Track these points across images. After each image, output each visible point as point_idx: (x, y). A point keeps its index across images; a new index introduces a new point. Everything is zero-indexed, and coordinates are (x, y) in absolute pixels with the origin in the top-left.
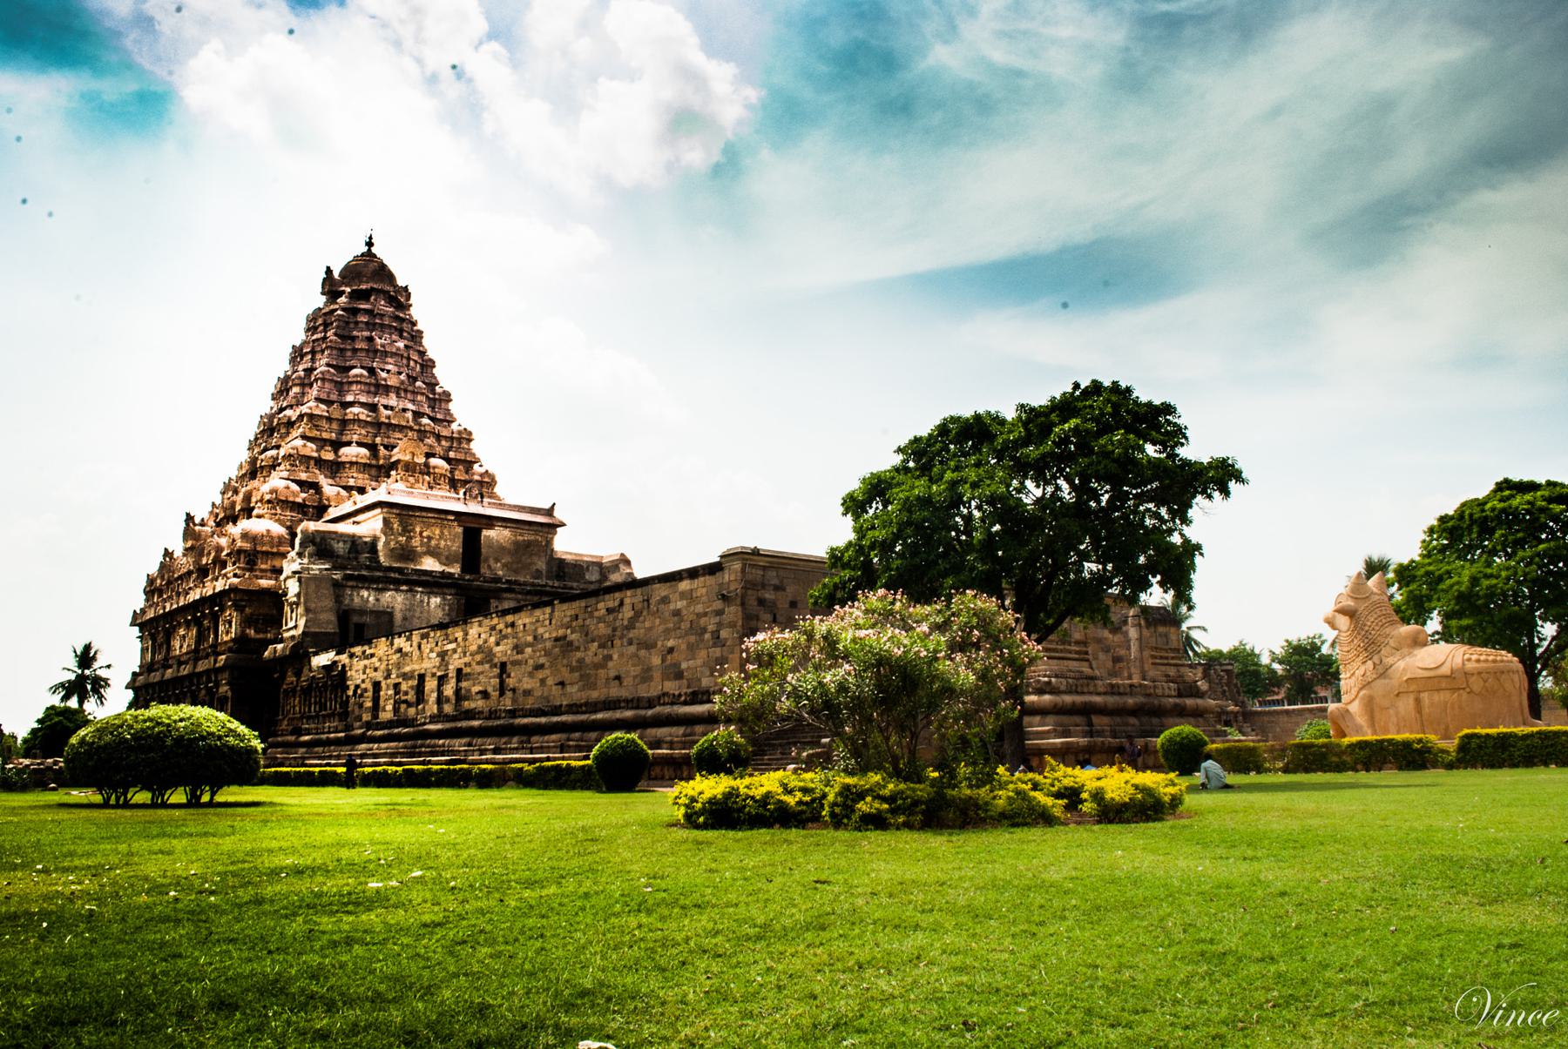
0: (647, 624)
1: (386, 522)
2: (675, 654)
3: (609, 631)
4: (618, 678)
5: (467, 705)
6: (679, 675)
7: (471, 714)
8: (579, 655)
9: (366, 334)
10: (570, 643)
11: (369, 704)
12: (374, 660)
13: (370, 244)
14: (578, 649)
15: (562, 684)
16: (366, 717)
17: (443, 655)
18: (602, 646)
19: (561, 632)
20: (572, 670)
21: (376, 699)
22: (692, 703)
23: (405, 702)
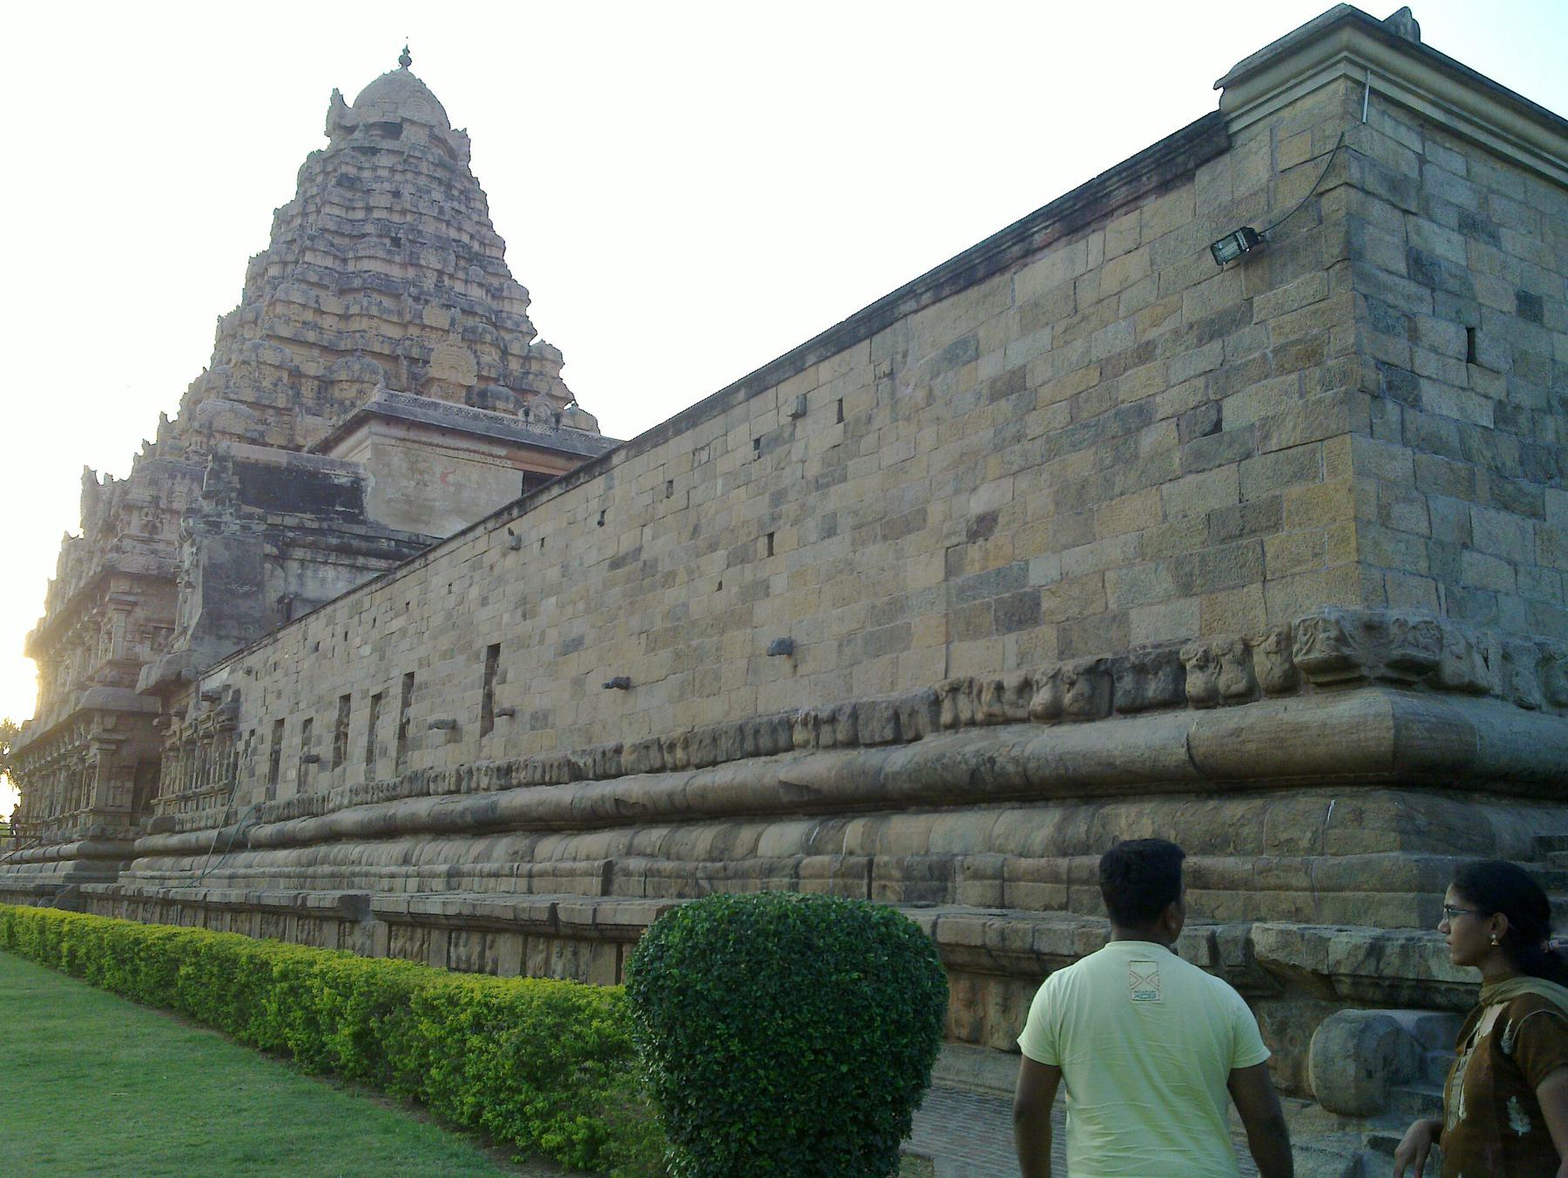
0: (889, 456)
1: (378, 452)
2: (1000, 536)
3: (763, 506)
4: (786, 648)
5: (420, 760)
6: (1021, 612)
7: (419, 786)
8: (672, 596)
9: (387, 186)
10: (649, 568)
11: (264, 768)
13: (405, 60)
14: (669, 578)
15: (624, 685)
16: (258, 796)
17: (381, 651)
19: (626, 544)
20: (654, 643)
22: (1087, 714)
23: (315, 759)
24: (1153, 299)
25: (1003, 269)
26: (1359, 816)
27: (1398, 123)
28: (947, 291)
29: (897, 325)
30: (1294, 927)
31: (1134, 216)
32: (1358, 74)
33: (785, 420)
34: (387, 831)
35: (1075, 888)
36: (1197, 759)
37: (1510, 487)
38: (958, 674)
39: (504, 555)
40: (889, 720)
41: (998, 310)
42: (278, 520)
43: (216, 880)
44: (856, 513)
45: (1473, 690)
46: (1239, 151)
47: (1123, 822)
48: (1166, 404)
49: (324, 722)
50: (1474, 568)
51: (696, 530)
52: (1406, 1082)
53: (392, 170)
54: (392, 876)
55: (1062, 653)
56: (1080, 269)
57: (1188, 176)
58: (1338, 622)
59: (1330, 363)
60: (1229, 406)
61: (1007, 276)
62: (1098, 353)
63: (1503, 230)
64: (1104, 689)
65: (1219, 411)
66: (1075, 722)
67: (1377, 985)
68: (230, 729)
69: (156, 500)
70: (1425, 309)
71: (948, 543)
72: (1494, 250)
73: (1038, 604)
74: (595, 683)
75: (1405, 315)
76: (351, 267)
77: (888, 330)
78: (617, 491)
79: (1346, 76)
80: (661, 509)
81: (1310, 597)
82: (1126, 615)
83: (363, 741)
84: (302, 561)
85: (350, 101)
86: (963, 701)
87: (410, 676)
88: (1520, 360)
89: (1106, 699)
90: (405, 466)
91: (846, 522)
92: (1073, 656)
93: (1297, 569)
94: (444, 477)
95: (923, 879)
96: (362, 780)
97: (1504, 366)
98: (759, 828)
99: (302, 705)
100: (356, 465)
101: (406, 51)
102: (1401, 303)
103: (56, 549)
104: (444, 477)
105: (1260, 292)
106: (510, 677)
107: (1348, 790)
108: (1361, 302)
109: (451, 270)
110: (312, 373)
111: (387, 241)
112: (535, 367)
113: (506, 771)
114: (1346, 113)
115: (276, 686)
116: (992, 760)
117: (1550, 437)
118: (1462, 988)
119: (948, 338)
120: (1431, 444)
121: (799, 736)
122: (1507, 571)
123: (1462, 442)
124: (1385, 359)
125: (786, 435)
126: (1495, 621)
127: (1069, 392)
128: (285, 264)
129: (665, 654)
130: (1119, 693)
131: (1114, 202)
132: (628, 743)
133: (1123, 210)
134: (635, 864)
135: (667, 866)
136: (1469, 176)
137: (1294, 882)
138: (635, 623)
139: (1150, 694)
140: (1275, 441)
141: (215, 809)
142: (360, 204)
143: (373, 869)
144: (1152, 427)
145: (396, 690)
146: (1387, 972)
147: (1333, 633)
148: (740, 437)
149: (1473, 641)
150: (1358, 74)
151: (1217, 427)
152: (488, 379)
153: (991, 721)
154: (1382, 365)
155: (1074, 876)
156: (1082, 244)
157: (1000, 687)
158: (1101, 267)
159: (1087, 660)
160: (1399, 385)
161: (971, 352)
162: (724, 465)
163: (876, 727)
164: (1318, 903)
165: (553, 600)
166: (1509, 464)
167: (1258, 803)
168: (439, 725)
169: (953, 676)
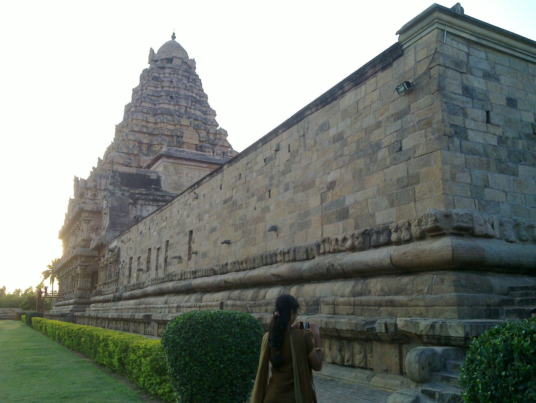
1: (165, 167)
2: (337, 189)
3: (267, 181)
4: (274, 229)
6: (343, 215)
7: (170, 278)
8: (241, 212)
9: (168, 79)
10: (235, 203)
11: (127, 273)
12: (131, 242)
13: (174, 37)
15: (228, 242)
16: (126, 283)
17: (159, 233)
18: (261, 199)
19: (228, 196)
21: (130, 271)
22: (363, 248)
24: (380, 107)
25: (336, 99)
26: (442, 281)
27: (458, 42)
28: (319, 107)
29: (305, 119)
30: (409, 319)
31: (374, 79)
32: (442, 27)
33: (273, 152)
34: (161, 293)
35: (356, 307)
36: (394, 263)
37: (504, 166)
38: (325, 236)
39: (193, 200)
40: (305, 252)
41: (334, 112)
42: (133, 191)
43: (112, 311)
44: (294, 182)
45: (487, 236)
46: (406, 55)
47: (372, 285)
48: (386, 141)
49: (144, 256)
50: (489, 194)
51: (248, 191)
52: (439, 371)
53: (170, 74)
54: (161, 308)
55: (356, 228)
56: (359, 98)
57: (390, 64)
58: (435, 215)
59: (434, 126)
60: (404, 141)
61: (337, 101)
62: (365, 126)
63: (501, 77)
64: (367, 240)
65: (401, 143)
66: (359, 251)
67: (434, 338)
68: (117, 261)
69: (95, 186)
70: (469, 105)
71: (321, 192)
72: (497, 84)
73: (348, 211)
74: (219, 243)
75: (461, 108)
76: (157, 107)
77: (303, 121)
78: (225, 178)
79: (438, 28)
80: (238, 183)
81: (428, 205)
82: (374, 214)
83: (155, 263)
84: (141, 205)
85: (156, 52)
86: (326, 245)
87: (168, 241)
88: (508, 122)
89: (368, 243)
90: (174, 172)
91: (291, 186)
92: (359, 229)
93: (425, 197)
94: (187, 175)
95: (312, 306)
96: (155, 276)
97: (501, 123)
98: (267, 289)
99: (137, 252)
100: (158, 172)
101: (174, 34)
102: (460, 104)
103: (67, 203)
104: (187, 175)
105: (413, 103)
106: (196, 240)
107: (442, 272)
108: (444, 105)
109: (190, 106)
110: (145, 142)
111: (169, 98)
112: (218, 136)
113: (195, 272)
114: (438, 40)
115: (130, 246)
116: (333, 265)
117: (520, 147)
118: (459, 339)
119: (321, 122)
120: (473, 152)
121: (279, 258)
122: (503, 194)
123: (485, 151)
124: (454, 124)
125: (273, 157)
126: (498, 212)
127: (356, 139)
128: (136, 107)
129: (240, 232)
130: (372, 241)
131: (369, 74)
132: (229, 262)
133: (371, 77)
134: (230, 302)
135: (238, 303)
136: (487, 59)
137: (420, 304)
138: (231, 221)
139: (381, 241)
140: (417, 153)
141: (113, 288)
142: (160, 86)
143: (156, 306)
144: (381, 150)
145: (164, 246)
146: (437, 334)
147: (433, 218)
148: (260, 158)
149: (487, 219)
150: (442, 27)
151: (401, 149)
152: (203, 141)
153: (335, 251)
154: (452, 126)
155: (355, 303)
156: (359, 89)
157: (337, 240)
158: (365, 96)
159: (362, 230)
160: (460, 132)
161: (327, 127)
162: (256, 168)
163: (301, 255)
164: (427, 311)
165: (208, 215)
166: (503, 157)
167: (413, 277)
168: (175, 257)
169: (324, 236)
